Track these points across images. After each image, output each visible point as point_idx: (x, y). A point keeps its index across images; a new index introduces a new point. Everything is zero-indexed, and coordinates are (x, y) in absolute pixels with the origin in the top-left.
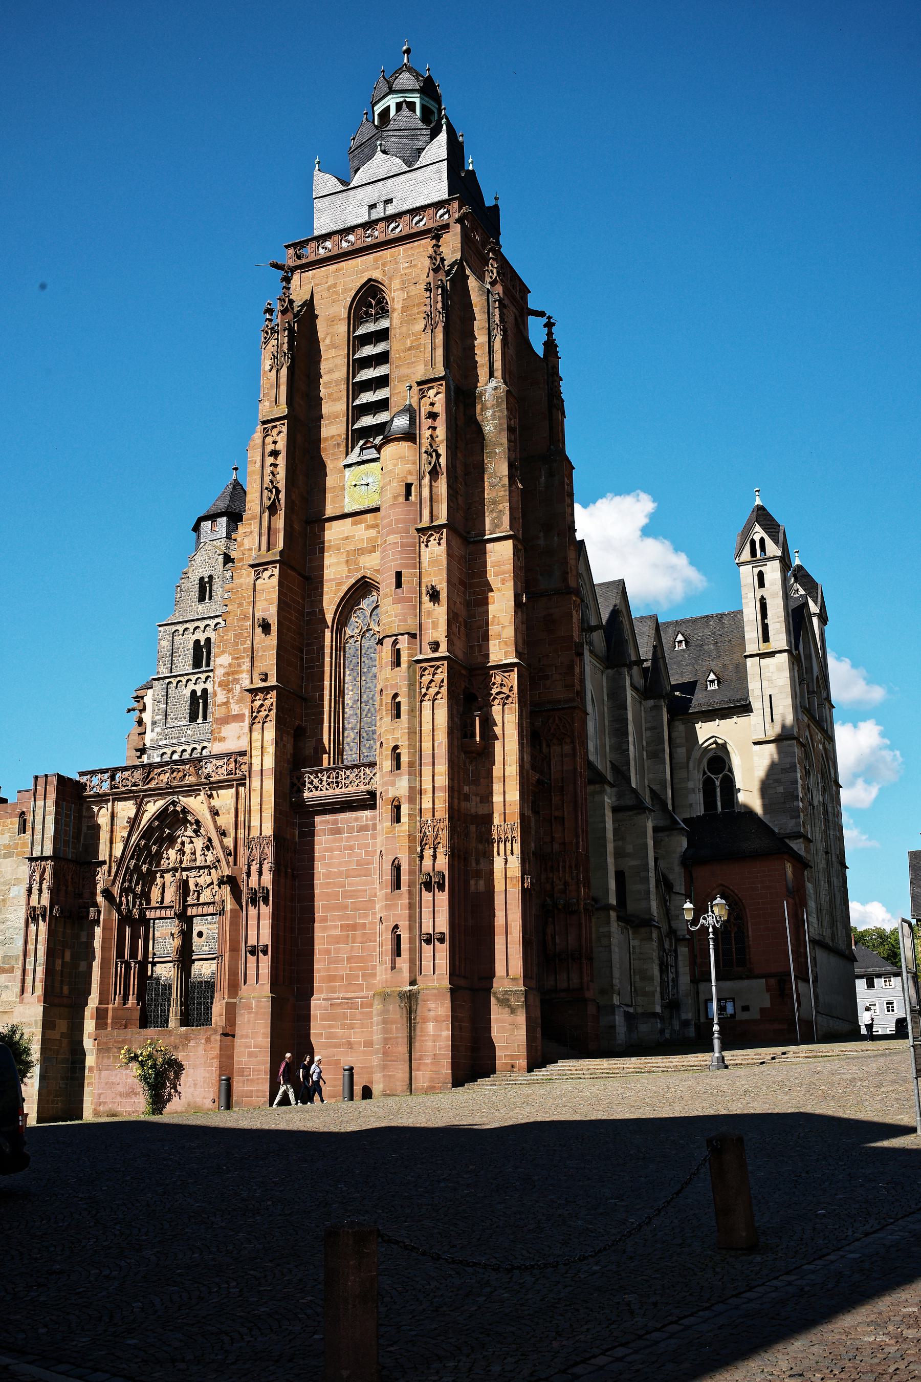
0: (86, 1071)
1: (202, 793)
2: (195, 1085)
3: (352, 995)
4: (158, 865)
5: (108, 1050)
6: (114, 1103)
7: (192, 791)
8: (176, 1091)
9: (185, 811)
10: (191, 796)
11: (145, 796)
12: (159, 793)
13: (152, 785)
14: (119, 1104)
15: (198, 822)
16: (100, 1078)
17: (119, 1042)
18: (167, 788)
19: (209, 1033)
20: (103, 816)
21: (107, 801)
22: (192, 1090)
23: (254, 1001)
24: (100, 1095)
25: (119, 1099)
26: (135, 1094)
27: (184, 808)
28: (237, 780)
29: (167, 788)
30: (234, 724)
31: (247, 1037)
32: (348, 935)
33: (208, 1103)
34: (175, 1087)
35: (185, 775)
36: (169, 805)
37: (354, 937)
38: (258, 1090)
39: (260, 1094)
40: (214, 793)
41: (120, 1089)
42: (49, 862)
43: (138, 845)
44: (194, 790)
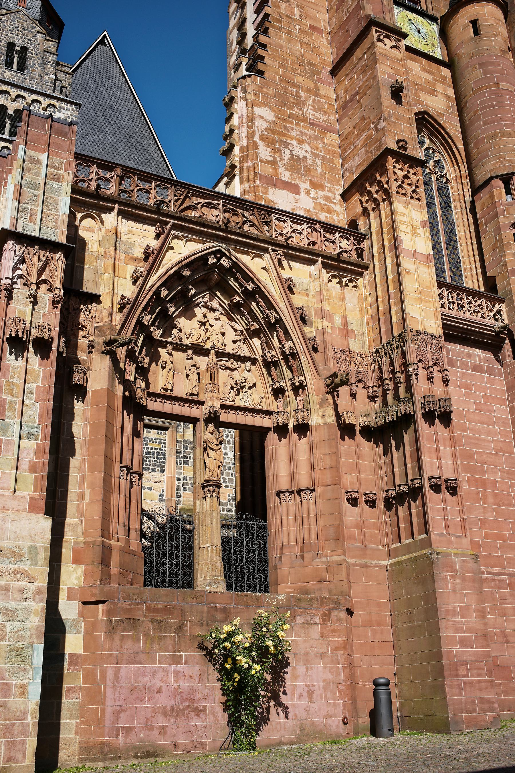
0: (66, 664)
1: (266, 256)
2: (310, 693)
3: (495, 570)
4: (167, 333)
5: (135, 624)
6: (151, 729)
7: (257, 246)
8: (279, 704)
9: (239, 271)
10: (247, 253)
11: (175, 227)
12: (199, 230)
13: (192, 214)
14: (163, 731)
15: (257, 293)
16: (117, 678)
17: (156, 610)
18: (219, 229)
19: (326, 607)
20: (88, 230)
21: (110, 210)
22: (305, 701)
23: (457, 560)
24: (117, 713)
25: (160, 721)
26: (198, 711)
27: (235, 265)
28: (323, 257)
29: (219, 229)
30: (284, 192)
31: (454, 614)
32: (478, 493)
33: (335, 724)
34: (275, 697)
35: (245, 223)
36: (210, 254)
37: (485, 496)
38: (482, 701)
39: (486, 706)
40: (285, 263)
41: (163, 701)
42: (60, 255)
43: (157, 293)
44: (254, 247)
